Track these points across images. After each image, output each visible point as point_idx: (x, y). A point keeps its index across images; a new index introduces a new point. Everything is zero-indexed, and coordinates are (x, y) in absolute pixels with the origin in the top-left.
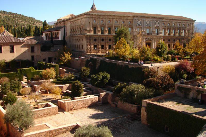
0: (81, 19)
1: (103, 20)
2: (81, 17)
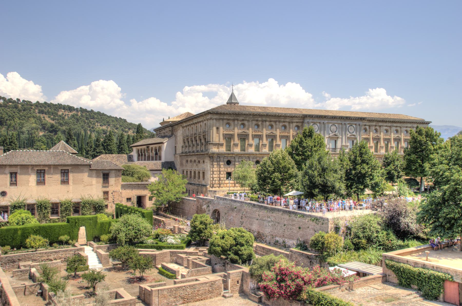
0: (202, 121)
1: (243, 124)
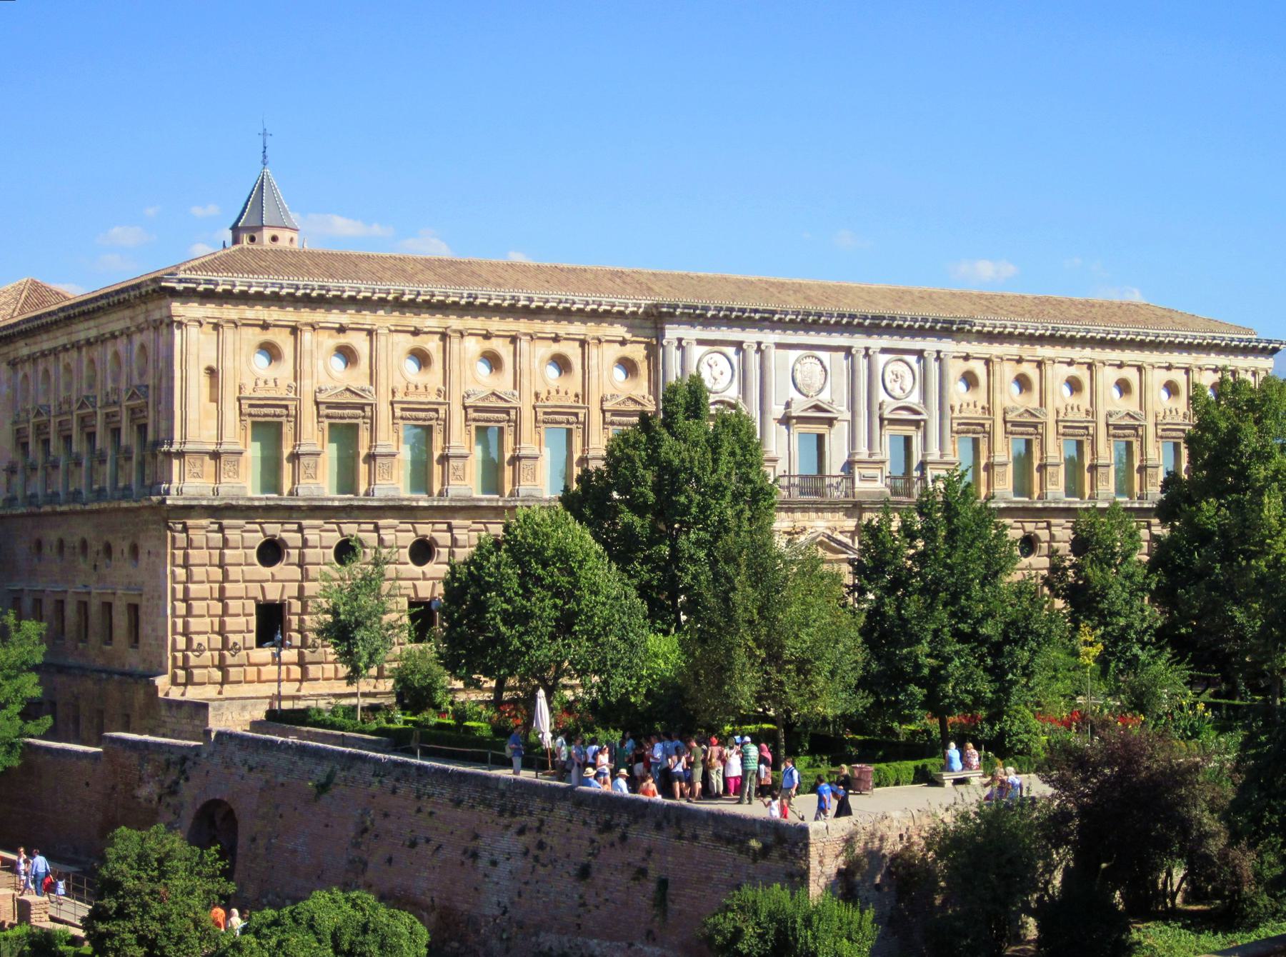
0: (126, 333)
2: (127, 313)
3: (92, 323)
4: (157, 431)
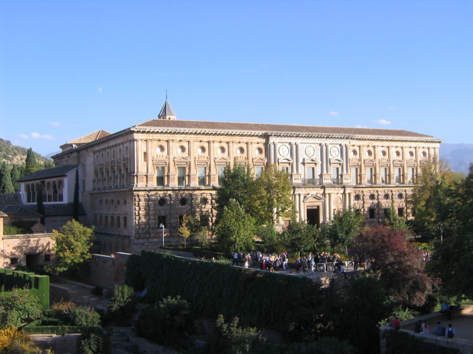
0: (123, 143)
2: (123, 138)
3: (114, 141)
4: (130, 170)
